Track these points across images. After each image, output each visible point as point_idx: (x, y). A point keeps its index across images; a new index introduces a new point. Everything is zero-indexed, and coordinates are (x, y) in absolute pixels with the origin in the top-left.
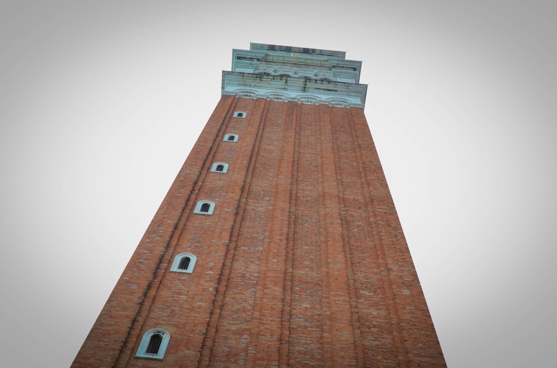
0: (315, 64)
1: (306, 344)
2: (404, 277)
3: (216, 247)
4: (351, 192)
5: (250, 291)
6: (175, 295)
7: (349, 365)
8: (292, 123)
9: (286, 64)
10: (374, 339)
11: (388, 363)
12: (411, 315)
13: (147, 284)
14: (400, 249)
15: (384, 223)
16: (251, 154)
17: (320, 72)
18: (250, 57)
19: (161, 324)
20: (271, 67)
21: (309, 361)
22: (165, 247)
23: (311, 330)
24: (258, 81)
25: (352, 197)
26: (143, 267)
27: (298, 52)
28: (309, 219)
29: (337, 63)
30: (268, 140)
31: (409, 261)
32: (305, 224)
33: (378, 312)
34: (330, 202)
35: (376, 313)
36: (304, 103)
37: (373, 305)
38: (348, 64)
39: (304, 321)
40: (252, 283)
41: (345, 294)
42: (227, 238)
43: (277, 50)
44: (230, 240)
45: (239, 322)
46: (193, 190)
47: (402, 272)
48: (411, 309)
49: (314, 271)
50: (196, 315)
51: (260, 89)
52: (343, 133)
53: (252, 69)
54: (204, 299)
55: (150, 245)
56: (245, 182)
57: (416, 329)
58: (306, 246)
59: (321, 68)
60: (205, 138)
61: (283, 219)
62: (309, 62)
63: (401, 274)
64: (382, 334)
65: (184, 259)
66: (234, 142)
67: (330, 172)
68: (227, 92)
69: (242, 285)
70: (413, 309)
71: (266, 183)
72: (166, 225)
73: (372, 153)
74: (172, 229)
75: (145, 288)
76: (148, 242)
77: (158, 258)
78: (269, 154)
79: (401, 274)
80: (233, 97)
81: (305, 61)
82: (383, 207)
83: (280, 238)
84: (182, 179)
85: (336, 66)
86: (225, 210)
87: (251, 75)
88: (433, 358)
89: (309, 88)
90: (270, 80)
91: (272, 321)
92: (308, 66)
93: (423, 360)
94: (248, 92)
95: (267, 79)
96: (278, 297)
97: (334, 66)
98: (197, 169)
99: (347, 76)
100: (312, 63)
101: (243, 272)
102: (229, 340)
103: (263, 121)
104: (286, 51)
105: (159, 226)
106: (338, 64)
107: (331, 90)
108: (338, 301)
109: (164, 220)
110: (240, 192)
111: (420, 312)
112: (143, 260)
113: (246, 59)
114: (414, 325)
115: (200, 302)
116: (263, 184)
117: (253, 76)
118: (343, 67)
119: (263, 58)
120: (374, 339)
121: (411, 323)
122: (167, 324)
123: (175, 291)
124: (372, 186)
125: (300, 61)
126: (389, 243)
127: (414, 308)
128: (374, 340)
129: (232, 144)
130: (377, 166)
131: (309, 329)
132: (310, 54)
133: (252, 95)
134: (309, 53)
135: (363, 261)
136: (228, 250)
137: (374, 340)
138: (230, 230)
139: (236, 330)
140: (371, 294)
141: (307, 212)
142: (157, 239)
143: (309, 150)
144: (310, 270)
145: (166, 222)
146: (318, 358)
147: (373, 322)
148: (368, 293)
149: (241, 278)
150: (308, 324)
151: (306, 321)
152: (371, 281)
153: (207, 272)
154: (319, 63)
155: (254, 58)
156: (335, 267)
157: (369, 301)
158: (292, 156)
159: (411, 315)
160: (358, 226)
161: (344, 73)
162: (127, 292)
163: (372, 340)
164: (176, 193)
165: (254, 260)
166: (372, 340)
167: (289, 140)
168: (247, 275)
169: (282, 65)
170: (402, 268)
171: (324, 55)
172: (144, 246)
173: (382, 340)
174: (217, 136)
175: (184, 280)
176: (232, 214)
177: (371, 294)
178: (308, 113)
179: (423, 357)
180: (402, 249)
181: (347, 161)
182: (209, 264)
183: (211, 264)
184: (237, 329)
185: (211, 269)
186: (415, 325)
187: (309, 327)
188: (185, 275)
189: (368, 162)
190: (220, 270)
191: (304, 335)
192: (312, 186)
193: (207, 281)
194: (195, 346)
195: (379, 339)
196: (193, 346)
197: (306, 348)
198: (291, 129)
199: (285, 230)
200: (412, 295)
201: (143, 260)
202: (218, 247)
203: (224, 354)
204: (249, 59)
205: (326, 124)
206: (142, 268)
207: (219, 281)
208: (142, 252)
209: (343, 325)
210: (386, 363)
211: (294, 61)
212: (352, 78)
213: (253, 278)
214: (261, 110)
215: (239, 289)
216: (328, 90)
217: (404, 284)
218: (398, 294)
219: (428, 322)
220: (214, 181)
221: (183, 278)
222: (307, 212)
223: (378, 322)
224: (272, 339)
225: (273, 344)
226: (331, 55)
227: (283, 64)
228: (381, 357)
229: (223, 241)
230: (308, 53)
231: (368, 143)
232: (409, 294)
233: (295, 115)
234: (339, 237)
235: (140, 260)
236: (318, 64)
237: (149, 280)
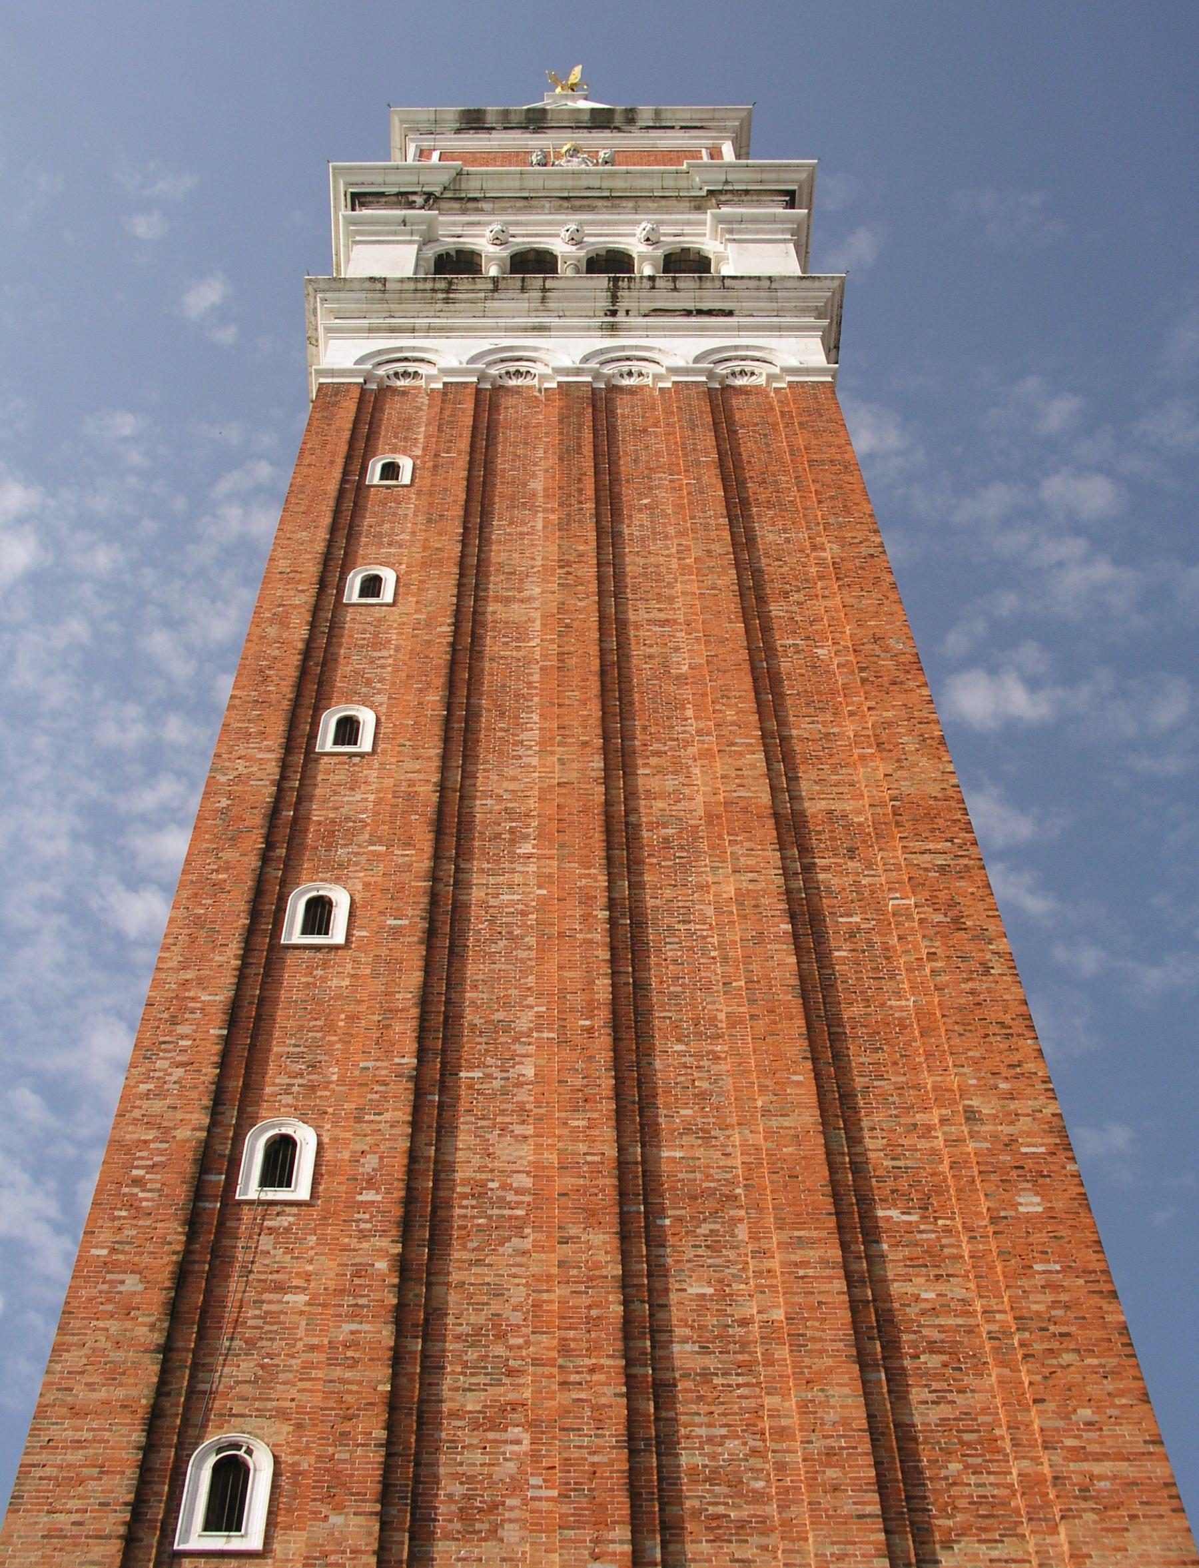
0: (642, 190)
1: (710, 1440)
2: (1020, 1140)
3: (376, 1088)
4: (816, 782)
5: (507, 1248)
6: (266, 1296)
7: (859, 1517)
8: (580, 490)
9: (534, 203)
10: (933, 1396)
11: (984, 1485)
12: (1049, 1297)
13: (170, 1268)
14: (1002, 1024)
15: (940, 918)
16: (448, 657)
17: (662, 223)
18: (395, 190)
19: (233, 1415)
20: (478, 223)
21: (726, 1504)
22: (206, 1108)
23: (723, 1385)
25: (823, 805)
26: (147, 1200)
27: (571, 128)
28: (679, 922)
29: (723, 178)
30: (502, 577)
31: (1036, 1073)
32: (669, 947)
33: (941, 1287)
34: (747, 845)
35: (932, 1295)
36: (614, 382)
37: (921, 1262)
38: (765, 176)
39: (698, 1353)
40: (511, 1217)
41: (824, 1234)
42: (411, 1046)
43: (493, 128)
44: (421, 1054)
45: (487, 1380)
46: (270, 844)
47: (1012, 1123)
48: (1050, 1272)
49: (714, 1142)
50: (348, 1375)
51: (448, 337)
52: (769, 508)
53: (410, 242)
54: (362, 1306)
55: (157, 1106)
56: (442, 787)
57: (1068, 1350)
58: (679, 1041)
59: (663, 203)
60: (280, 606)
61: (591, 941)
62: (619, 183)
63: (1010, 1129)
64: (957, 1374)
65: (275, 1142)
66: (381, 605)
67: (736, 705)
68: (332, 373)
69: (481, 1229)
70: (1058, 1272)
71: (514, 779)
72: (198, 1015)
73: (880, 596)
74: (221, 1028)
75: (168, 1284)
76: (147, 1095)
77: (190, 1155)
78: (514, 644)
79: (1010, 1129)
80: (356, 394)
81: (605, 184)
82: (931, 846)
83: (587, 1023)
84: (224, 802)
85: (720, 192)
86: (388, 922)
87: (411, 286)
88: (1129, 1460)
89: (627, 312)
90: (482, 295)
91: (592, 1370)
92: (617, 202)
93: (1097, 1468)
94: (406, 359)
95: (473, 291)
96: (604, 1272)
97: (711, 192)
98: (270, 750)
99: (765, 232)
100: (631, 189)
101: (478, 1176)
102: (462, 1454)
103: (478, 489)
104: (526, 128)
105: (174, 1021)
106: (726, 182)
107: (710, 313)
108: (805, 1264)
109: (187, 994)
110: (431, 836)
111: (1081, 1282)
112: (141, 1172)
113: (384, 200)
114: (1061, 1335)
115: (353, 1322)
116: (506, 785)
117: (420, 286)
118: (747, 192)
119: (445, 188)
120: (933, 1396)
121: (1052, 1328)
122: (257, 1410)
123: (263, 1277)
124: (890, 751)
125: (584, 183)
126: (963, 1001)
127: (1058, 1267)
128: (933, 1403)
129: (378, 613)
130: (902, 659)
131: (716, 1381)
132: (618, 129)
133: (423, 369)
134: (615, 128)
135: (876, 1083)
136: (419, 1094)
137: (933, 1403)
138: (415, 1012)
139: (480, 1412)
140: (914, 1218)
141: (668, 893)
142: (174, 1078)
143: (653, 604)
144: (700, 1142)
145: (193, 999)
146: (754, 1491)
147: (925, 1332)
148: (903, 1213)
149: (474, 1202)
150: (711, 1363)
151: (705, 1350)
152: (909, 1163)
153: (359, 1198)
154: (657, 184)
155: (414, 193)
156: (786, 1124)
157: (907, 1246)
158: (594, 650)
159: (1049, 1297)
160: (852, 934)
161: (755, 220)
162: (110, 1307)
163: (927, 1403)
164: (213, 871)
165: (508, 1119)
166: (927, 1403)
167: (579, 574)
168: (491, 1185)
169: (520, 209)
170: (1013, 1105)
171: (673, 128)
172: (137, 1113)
173: (960, 1399)
174: (322, 584)
175: (288, 1230)
176: (415, 939)
177: (914, 1218)
178: (634, 430)
179: (1098, 1458)
180: (1008, 1021)
181: (791, 642)
182: (362, 1160)
183: (370, 1163)
184: (484, 1406)
185: (371, 1183)
186: (1068, 1335)
187: (717, 1374)
188: (287, 1209)
189: (869, 642)
190: (402, 1185)
191: (703, 1408)
192: (675, 773)
193: (363, 1236)
194: (358, 1494)
195: (949, 1396)
196: (352, 1494)
197: (713, 1457)
198: (579, 522)
199: (603, 985)
200: (1050, 1215)
201: (141, 1172)
202: (382, 1088)
203: (454, 1508)
204: (394, 199)
205: (705, 479)
206: (144, 1204)
207: (406, 1226)
208: (135, 1136)
209: (829, 1362)
210: (978, 1485)
211: (562, 189)
212: (785, 241)
213: (511, 1197)
214: (464, 444)
215: (471, 1245)
216: (700, 312)
217: (1020, 1172)
218: (1002, 1214)
219: (1108, 1318)
220: (336, 793)
221: (284, 1221)
222: (668, 893)
223: (941, 1329)
224: (600, 1441)
225: (605, 1459)
226: (699, 124)
227: (520, 204)
228: (960, 1466)
229: (397, 1060)
230: (609, 128)
231: (864, 551)
232: (1040, 1209)
233: (588, 450)
234: (789, 997)
235: (135, 1172)
236: (652, 190)
237: (174, 1253)
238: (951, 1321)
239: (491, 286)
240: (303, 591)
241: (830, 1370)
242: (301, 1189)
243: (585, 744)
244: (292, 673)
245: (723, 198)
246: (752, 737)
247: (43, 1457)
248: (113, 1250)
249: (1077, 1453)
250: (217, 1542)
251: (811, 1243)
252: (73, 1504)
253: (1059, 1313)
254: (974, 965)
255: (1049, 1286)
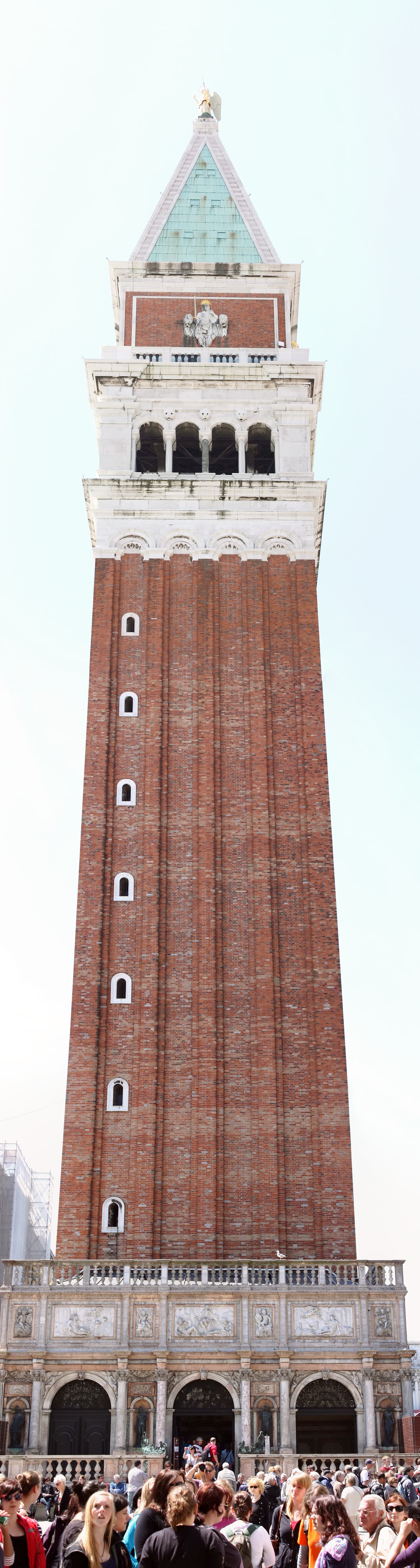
9: (186, 382)
24: (145, 493)
63: (325, 980)
79: (325, 980)
108: (264, 1027)
118: (290, 379)
200: (332, 1011)
238: (302, 1042)
239: (167, 484)
240: (103, 713)
241: (268, 1061)
242: (128, 1000)
243: (208, 805)
244: (104, 764)
245: (278, 382)
246: (264, 801)
247: (72, 1088)
248: (80, 1025)
249: (327, 1087)
250: (117, 1108)
251: (266, 1020)
252: (82, 1102)
253: (329, 1043)
254: (324, 913)
255: (328, 1035)
